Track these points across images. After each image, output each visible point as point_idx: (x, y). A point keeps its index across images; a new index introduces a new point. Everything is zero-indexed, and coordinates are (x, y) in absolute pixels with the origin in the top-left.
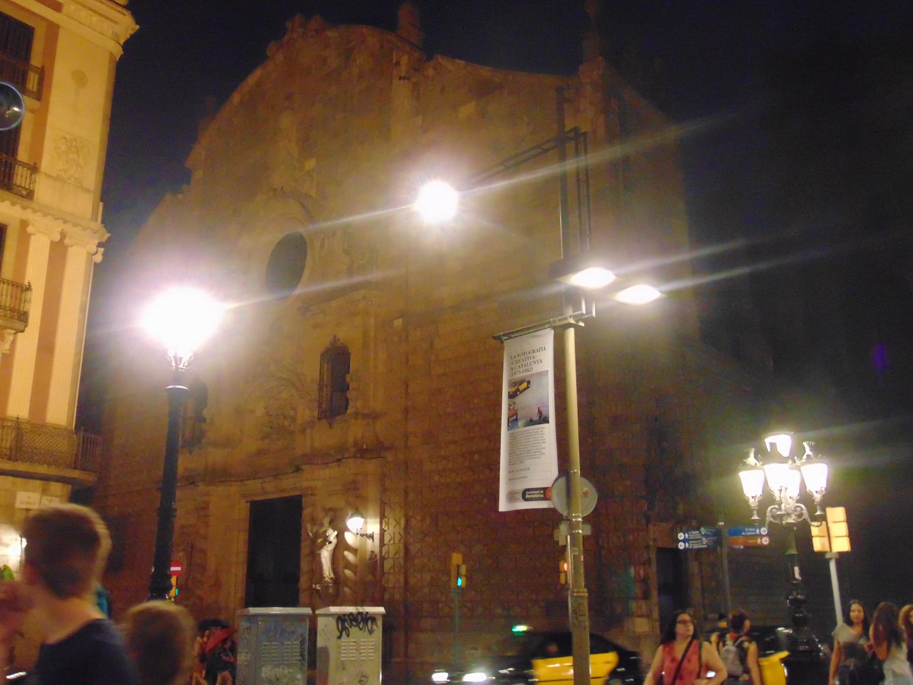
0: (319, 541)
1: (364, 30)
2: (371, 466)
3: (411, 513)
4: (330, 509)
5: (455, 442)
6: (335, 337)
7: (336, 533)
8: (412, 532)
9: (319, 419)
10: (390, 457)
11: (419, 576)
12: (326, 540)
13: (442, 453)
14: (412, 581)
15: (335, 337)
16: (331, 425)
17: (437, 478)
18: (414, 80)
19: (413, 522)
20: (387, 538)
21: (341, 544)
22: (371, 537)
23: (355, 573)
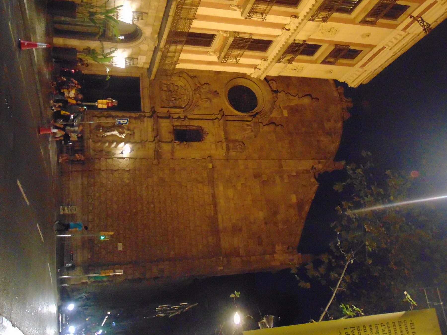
0: (121, 130)
1: (338, 144)
2: (151, 153)
3: (131, 172)
4: (134, 133)
5: (159, 195)
6: (208, 134)
7: (123, 137)
8: (123, 173)
9: (173, 125)
10: (155, 162)
11: (105, 176)
12: (121, 133)
13: (155, 188)
14: (103, 173)
15: (208, 134)
16: (170, 132)
17: (145, 186)
18: (311, 171)
19: (127, 173)
20: (121, 160)
21: (119, 141)
22: (122, 153)
23: (107, 147)
